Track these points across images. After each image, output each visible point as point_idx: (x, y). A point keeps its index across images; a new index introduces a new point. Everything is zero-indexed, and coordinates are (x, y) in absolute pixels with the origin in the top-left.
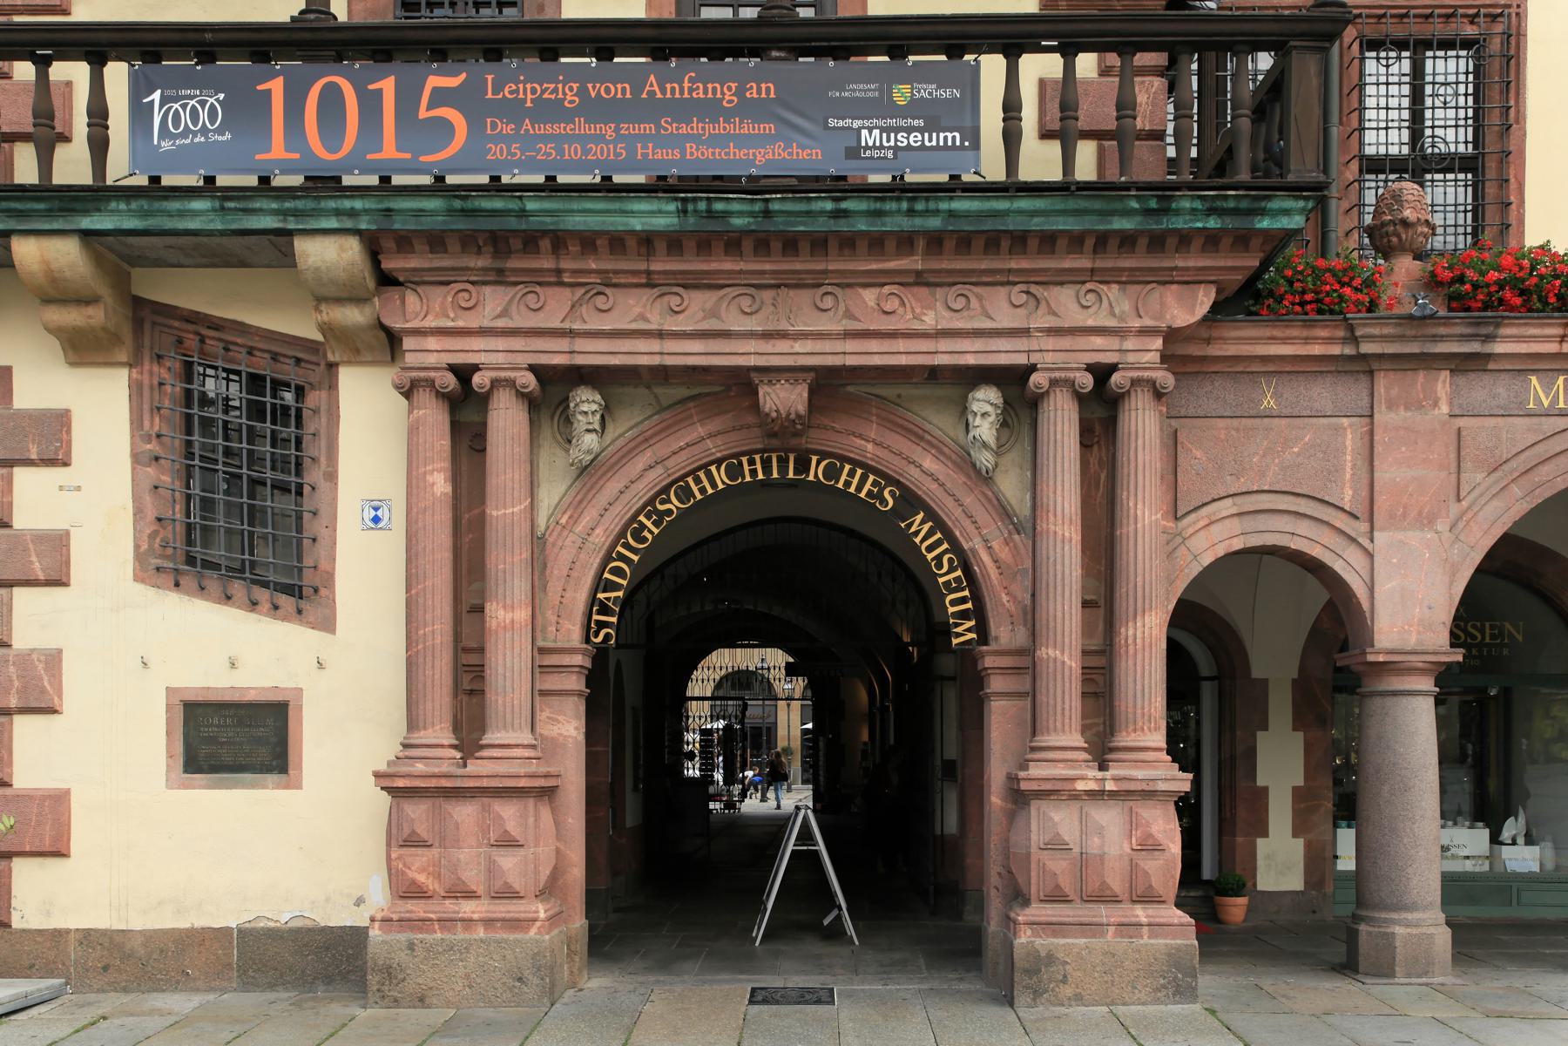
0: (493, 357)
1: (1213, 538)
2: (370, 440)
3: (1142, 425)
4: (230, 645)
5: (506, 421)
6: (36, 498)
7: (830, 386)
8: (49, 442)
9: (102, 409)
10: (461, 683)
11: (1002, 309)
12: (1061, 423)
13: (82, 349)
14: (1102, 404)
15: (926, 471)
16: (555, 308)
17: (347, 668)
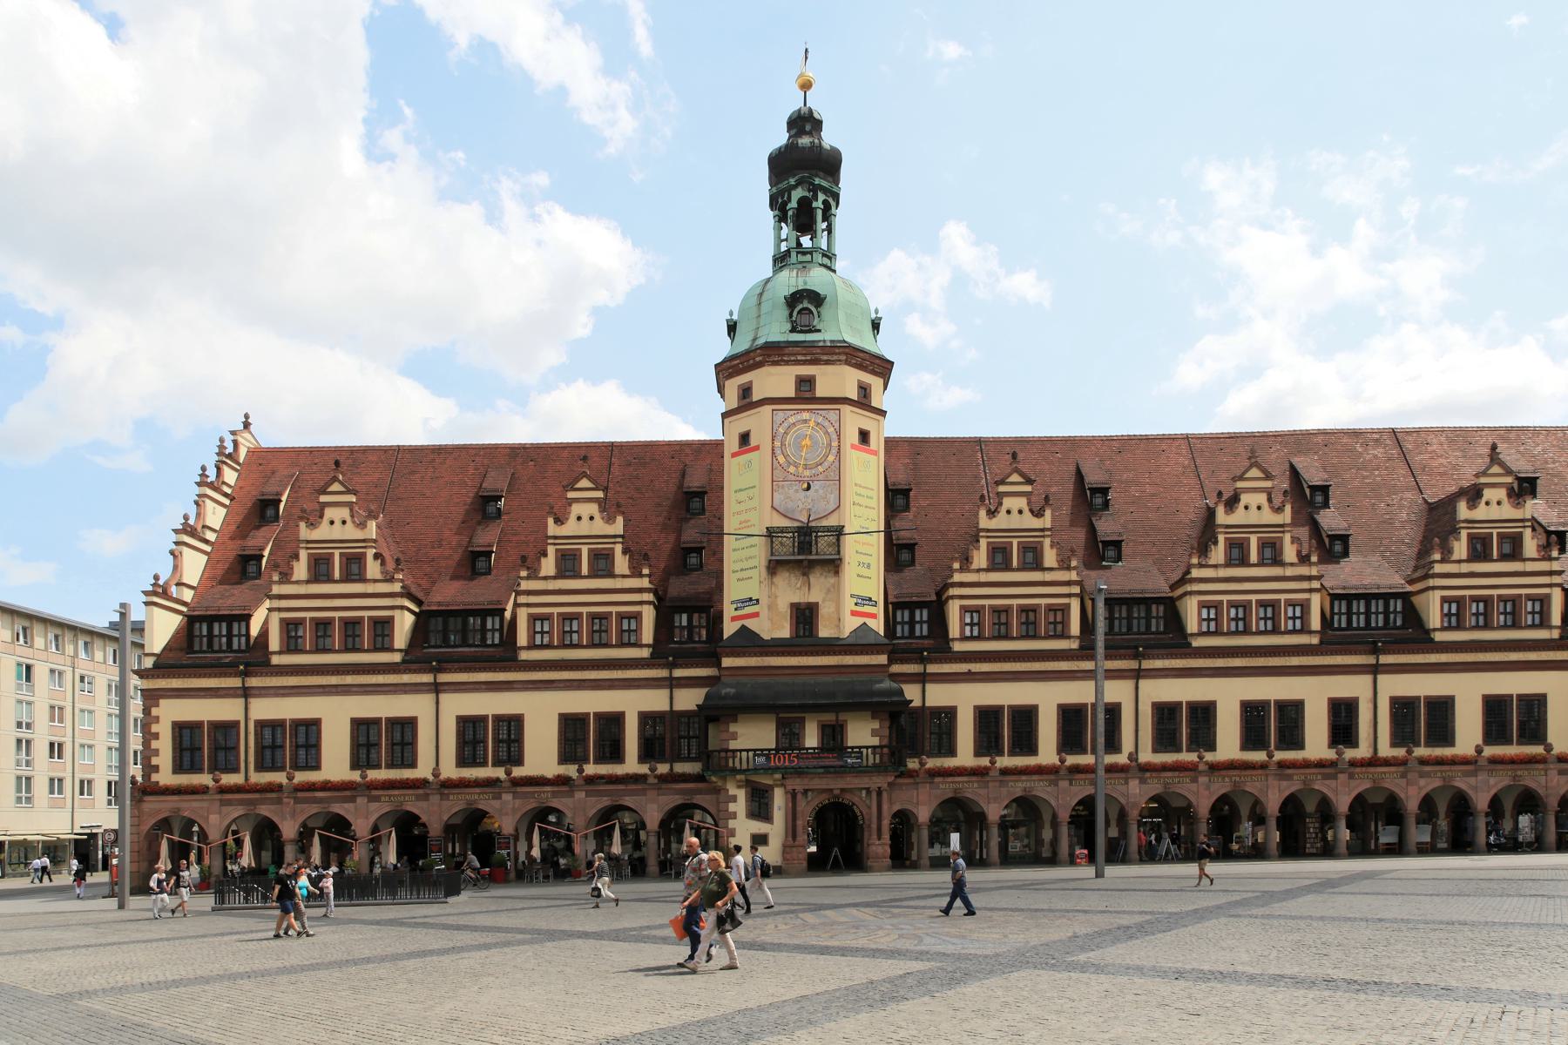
0: (799, 788)
1: (896, 808)
2: (779, 799)
3: (885, 795)
4: (759, 827)
5: (799, 796)
6: (732, 807)
7: (843, 790)
8: (734, 799)
9: (741, 795)
10: (792, 831)
11: (866, 780)
12: (874, 795)
13: (739, 787)
14: (879, 793)
15: (856, 800)
16: (806, 781)
17: (776, 830)
